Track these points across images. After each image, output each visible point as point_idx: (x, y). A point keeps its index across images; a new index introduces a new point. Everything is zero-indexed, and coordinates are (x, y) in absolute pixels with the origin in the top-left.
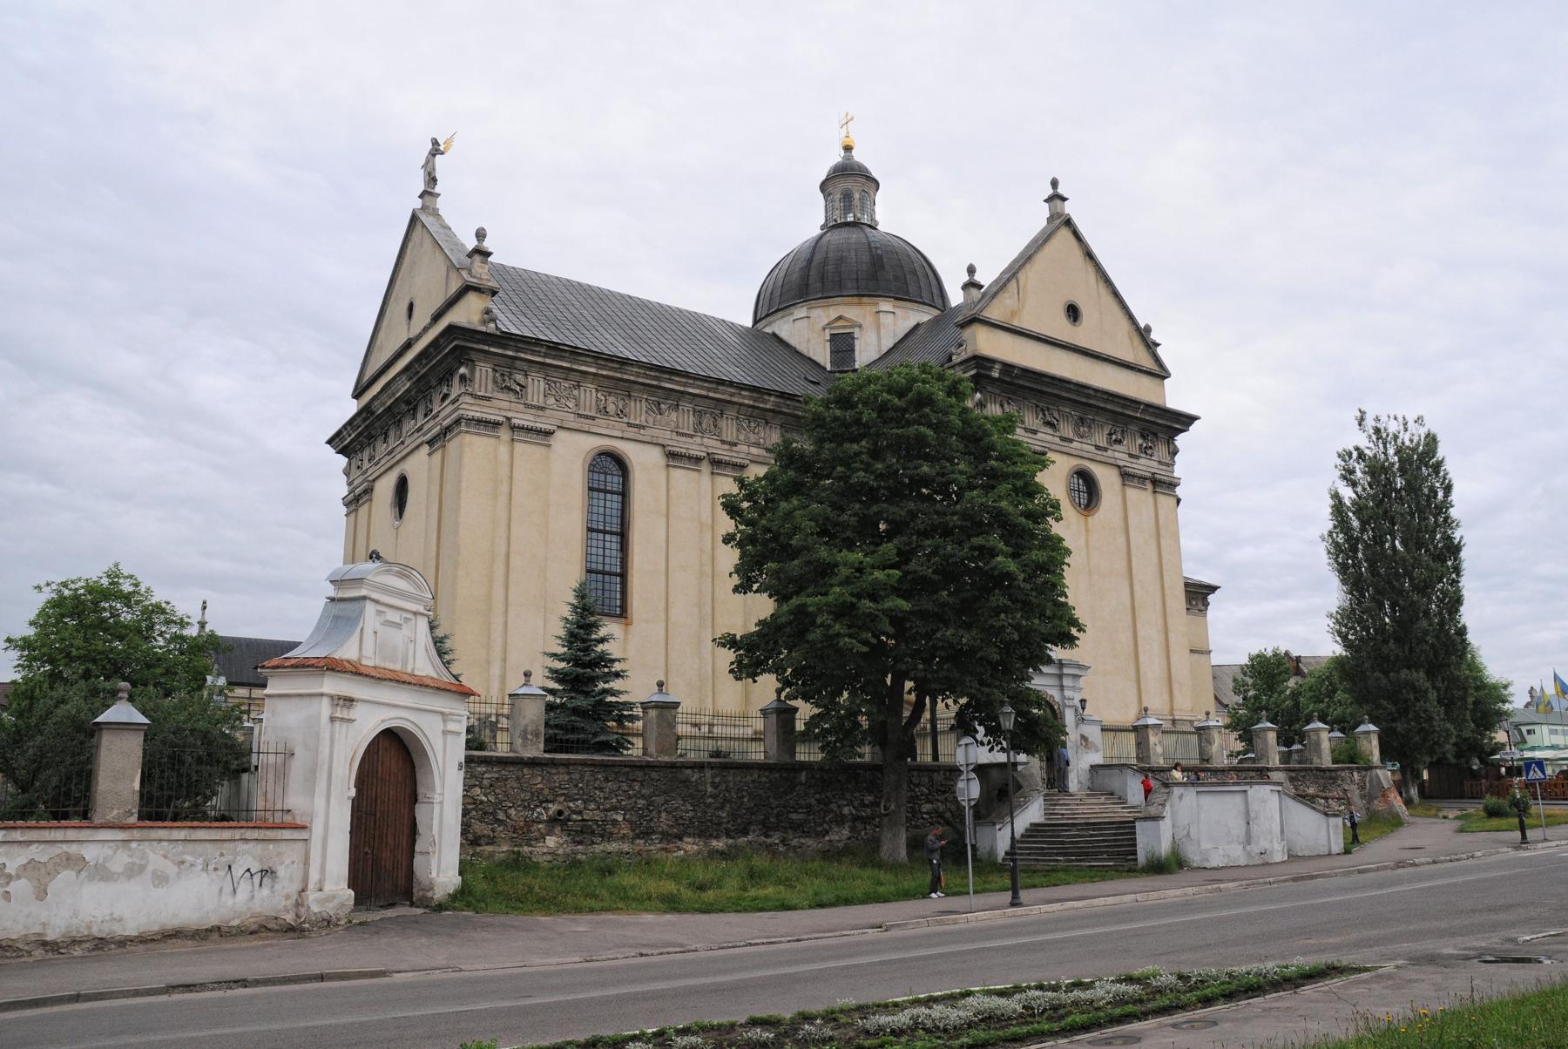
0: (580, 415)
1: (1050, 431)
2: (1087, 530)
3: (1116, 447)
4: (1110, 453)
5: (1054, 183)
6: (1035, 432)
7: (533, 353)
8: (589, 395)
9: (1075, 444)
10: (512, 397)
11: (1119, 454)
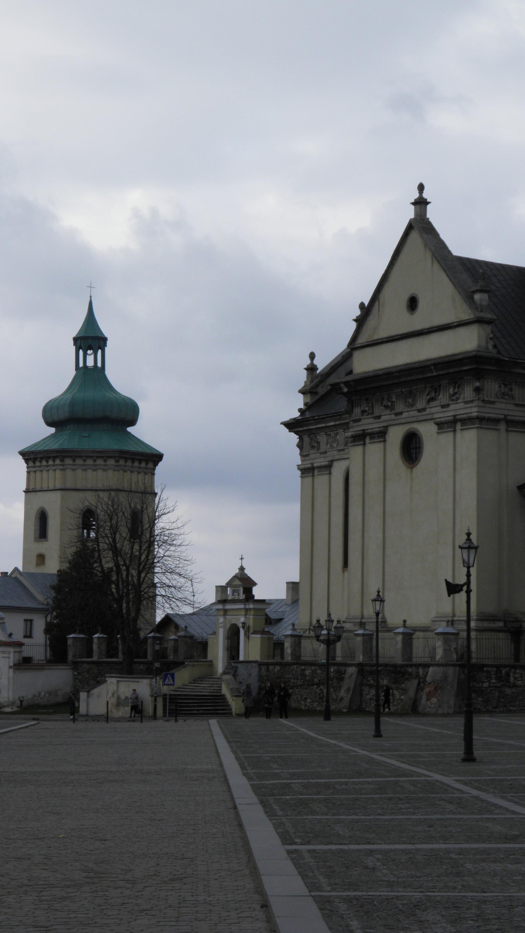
1: (388, 412)
3: (432, 404)
4: (428, 411)
5: (421, 188)
7: (312, 424)
9: (405, 415)
10: (315, 451)
11: (436, 411)
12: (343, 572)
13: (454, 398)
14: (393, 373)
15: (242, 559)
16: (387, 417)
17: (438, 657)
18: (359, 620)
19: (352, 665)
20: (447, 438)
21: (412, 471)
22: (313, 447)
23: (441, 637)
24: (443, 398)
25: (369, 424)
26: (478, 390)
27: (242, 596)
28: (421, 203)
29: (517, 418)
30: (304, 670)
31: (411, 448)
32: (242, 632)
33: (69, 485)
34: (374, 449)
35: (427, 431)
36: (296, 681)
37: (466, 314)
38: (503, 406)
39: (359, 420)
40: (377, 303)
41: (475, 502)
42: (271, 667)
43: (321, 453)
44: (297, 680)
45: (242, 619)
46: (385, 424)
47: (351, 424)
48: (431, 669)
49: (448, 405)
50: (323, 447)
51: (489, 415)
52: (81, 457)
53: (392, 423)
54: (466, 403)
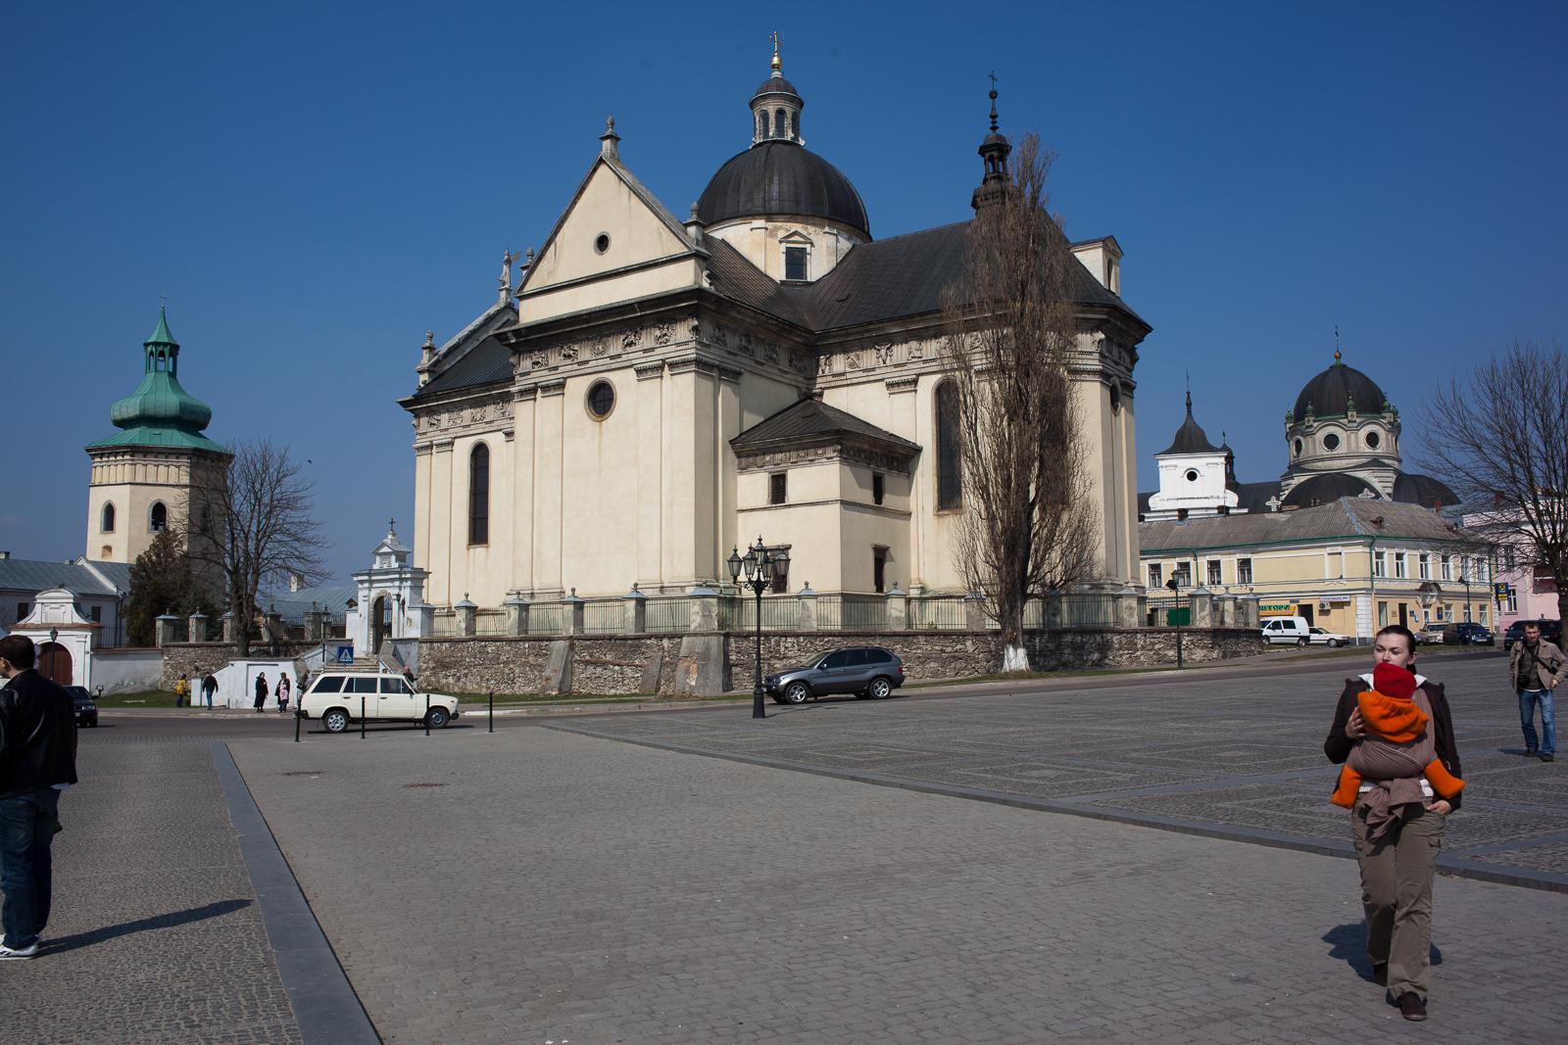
0: (464, 427)
1: (569, 361)
2: (601, 434)
3: (629, 349)
4: (624, 357)
6: (556, 368)
8: (467, 413)
10: (434, 428)
11: (636, 356)
12: (468, 549)
13: (664, 339)
14: (582, 315)
15: (392, 523)
17: (692, 626)
18: (530, 592)
19: (560, 639)
20: (651, 385)
21: (601, 425)
22: (432, 424)
23: (698, 601)
24: (647, 339)
25: (542, 376)
26: (695, 329)
27: (395, 565)
29: (730, 366)
30: (486, 646)
31: (601, 400)
32: (395, 605)
33: (138, 480)
36: (473, 659)
37: (678, 249)
38: (717, 351)
39: (528, 373)
40: (552, 246)
41: (693, 453)
42: (436, 645)
43: (442, 430)
44: (475, 658)
45: (396, 591)
46: (565, 375)
47: (517, 378)
48: (684, 639)
49: (653, 349)
50: (444, 424)
51: (707, 360)
52: (152, 453)
53: (574, 373)
54: (678, 344)
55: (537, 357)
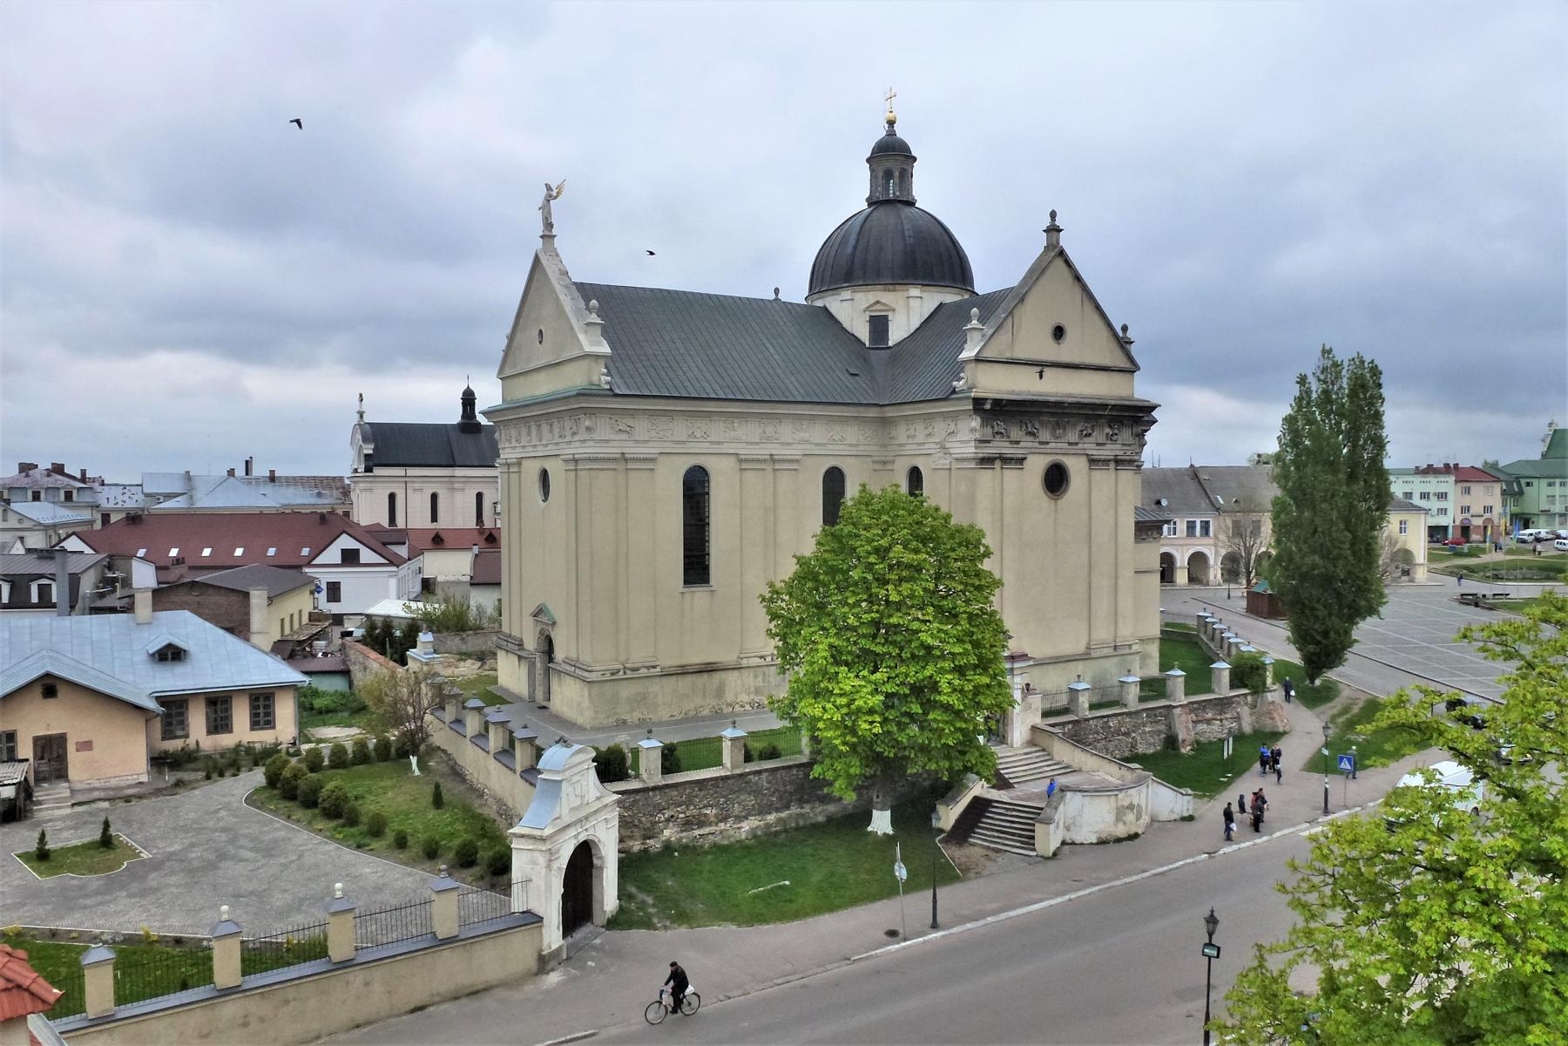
2: (1056, 511)
3: (1087, 440)
5: (1053, 215)
10: (624, 436)
11: (1089, 446)
16: (1028, 443)
24: (1099, 435)
28: (1053, 230)
31: (1056, 480)
34: (1011, 475)
35: (1076, 467)
55: (1000, 426)
